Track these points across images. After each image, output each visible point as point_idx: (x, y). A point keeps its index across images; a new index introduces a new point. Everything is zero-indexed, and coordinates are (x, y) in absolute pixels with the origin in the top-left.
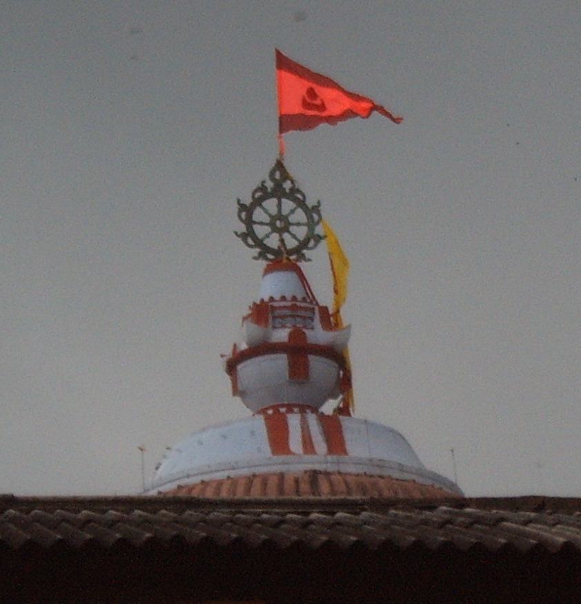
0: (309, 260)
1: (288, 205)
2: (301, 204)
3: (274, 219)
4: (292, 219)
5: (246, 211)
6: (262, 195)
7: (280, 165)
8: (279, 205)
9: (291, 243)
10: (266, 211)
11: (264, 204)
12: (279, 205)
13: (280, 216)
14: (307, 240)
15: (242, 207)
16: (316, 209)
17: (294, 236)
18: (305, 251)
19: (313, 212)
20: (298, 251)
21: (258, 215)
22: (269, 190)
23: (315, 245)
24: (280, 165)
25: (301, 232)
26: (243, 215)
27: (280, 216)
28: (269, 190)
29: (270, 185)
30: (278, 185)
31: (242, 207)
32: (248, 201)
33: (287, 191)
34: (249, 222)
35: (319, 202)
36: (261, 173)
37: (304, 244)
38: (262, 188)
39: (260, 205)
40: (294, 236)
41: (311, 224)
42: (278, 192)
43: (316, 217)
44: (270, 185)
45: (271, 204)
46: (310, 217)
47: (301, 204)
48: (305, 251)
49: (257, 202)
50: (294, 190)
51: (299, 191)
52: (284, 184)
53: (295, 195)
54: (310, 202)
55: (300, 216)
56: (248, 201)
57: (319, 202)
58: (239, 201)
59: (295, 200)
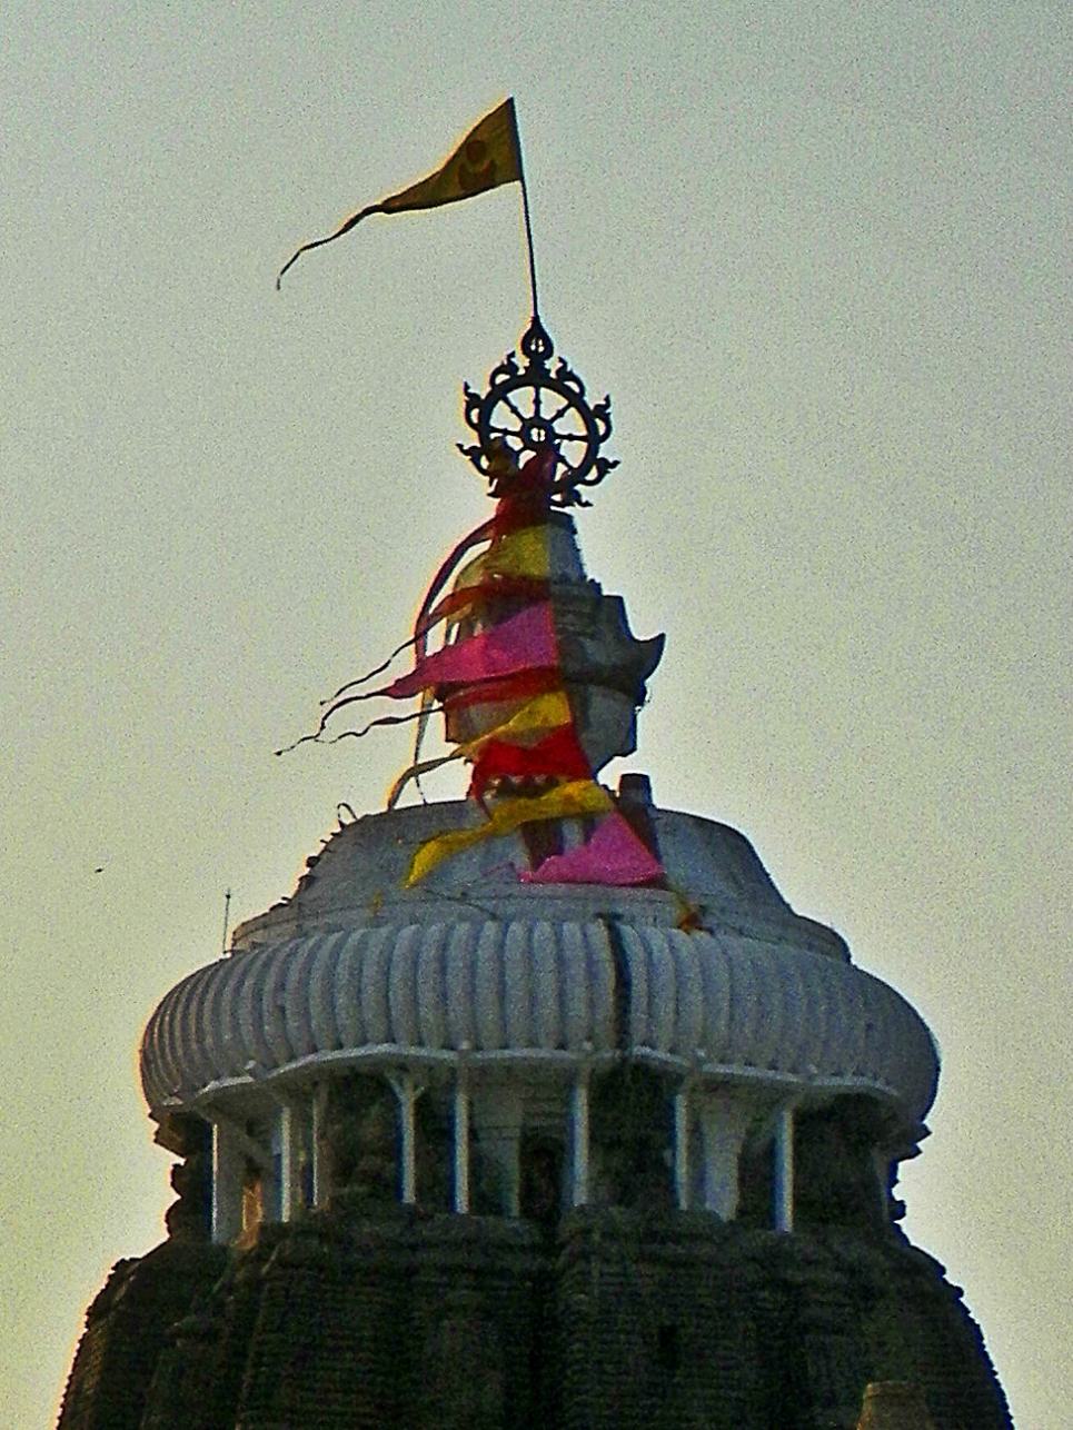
0: (587, 504)
1: (552, 401)
2: (576, 400)
3: (528, 425)
4: (559, 427)
5: (479, 407)
6: (507, 380)
7: (536, 331)
13: (537, 421)
15: (473, 401)
16: (602, 411)
19: (595, 416)
21: (501, 418)
22: (522, 372)
24: (536, 331)
26: (475, 413)
28: (522, 372)
29: (522, 362)
30: (537, 360)
31: (473, 401)
32: (483, 391)
34: (483, 427)
35: (607, 399)
36: (507, 342)
38: (509, 367)
44: (522, 362)
45: (522, 397)
47: (576, 400)
49: (499, 393)
50: (565, 374)
52: (546, 362)
53: (563, 382)
55: (572, 423)
56: (483, 391)
57: (607, 399)
58: (467, 387)
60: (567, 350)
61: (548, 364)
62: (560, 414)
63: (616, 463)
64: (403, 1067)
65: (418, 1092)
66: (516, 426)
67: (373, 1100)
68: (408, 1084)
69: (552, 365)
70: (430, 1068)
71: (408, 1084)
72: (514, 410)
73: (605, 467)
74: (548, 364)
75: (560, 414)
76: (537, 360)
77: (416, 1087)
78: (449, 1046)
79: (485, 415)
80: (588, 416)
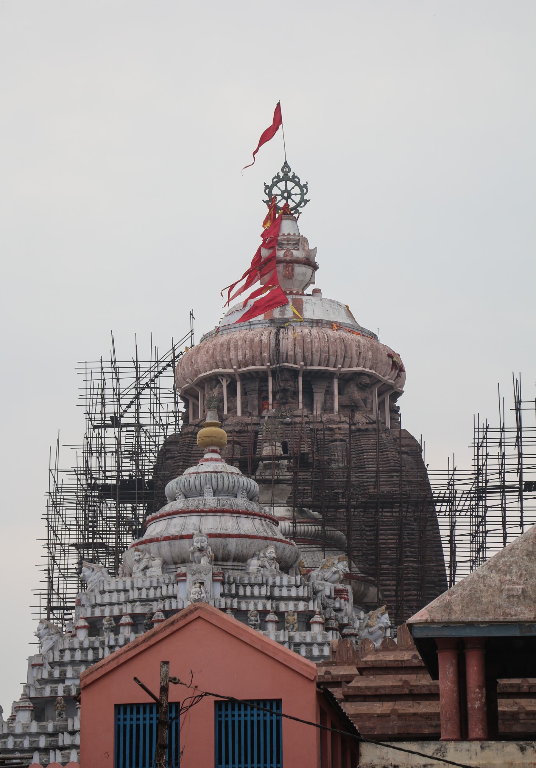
1: (290, 185)
2: (298, 184)
3: (283, 192)
4: (293, 192)
5: (268, 189)
6: (277, 180)
7: (286, 165)
8: (286, 185)
9: (292, 205)
10: (279, 188)
11: (278, 185)
12: (286, 185)
13: (286, 191)
14: (300, 202)
15: (267, 187)
16: (305, 186)
17: (293, 201)
18: (299, 208)
19: (304, 188)
20: (295, 208)
21: (275, 191)
22: (281, 177)
23: (304, 205)
24: (286, 165)
25: (297, 199)
26: (267, 191)
27: (286, 191)
28: (281, 177)
29: (281, 175)
30: (286, 174)
31: (267, 187)
32: (269, 184)
33: (291, 177)
34: (270, 194)
35: (307, 182)
36: (277, 169)
37: (298, 205)
38: (278, 176)
39: (276, 186)
40: (293, 201)
41: (303, 194)
42: (286, 178)
43: (305, 190)
44: (281, 175)
45: (282, 185)
46: (302, 191)
47: (298, 184)
48: (299, 208)
49: (275, 184)
50: (294, 176)
51: (297, 177)
53: (295, 179)
54: (302, 183)
55: (297, 190)
56: (269, 184)
57: (307, 182)
58: (265, 184)
59: (294, 182)
60: (295, 169)
61: (289, 174)
62: (293, 188)
63: (309, 200)
64: (222, 375)
65: (228, 382)
66: (280, 193)
67: (216, 386)
68: (225, 380)
69: (290, 175)
70: (229, 375)
71: (225, 380)
72: (279, 188)
73: (306, 202)
74: (289, 174)
75: (293, 188)
76: (286, 174)
77: (227, 381)
78: (232, 368)
79: (271, 191)
80: (301, 188)
